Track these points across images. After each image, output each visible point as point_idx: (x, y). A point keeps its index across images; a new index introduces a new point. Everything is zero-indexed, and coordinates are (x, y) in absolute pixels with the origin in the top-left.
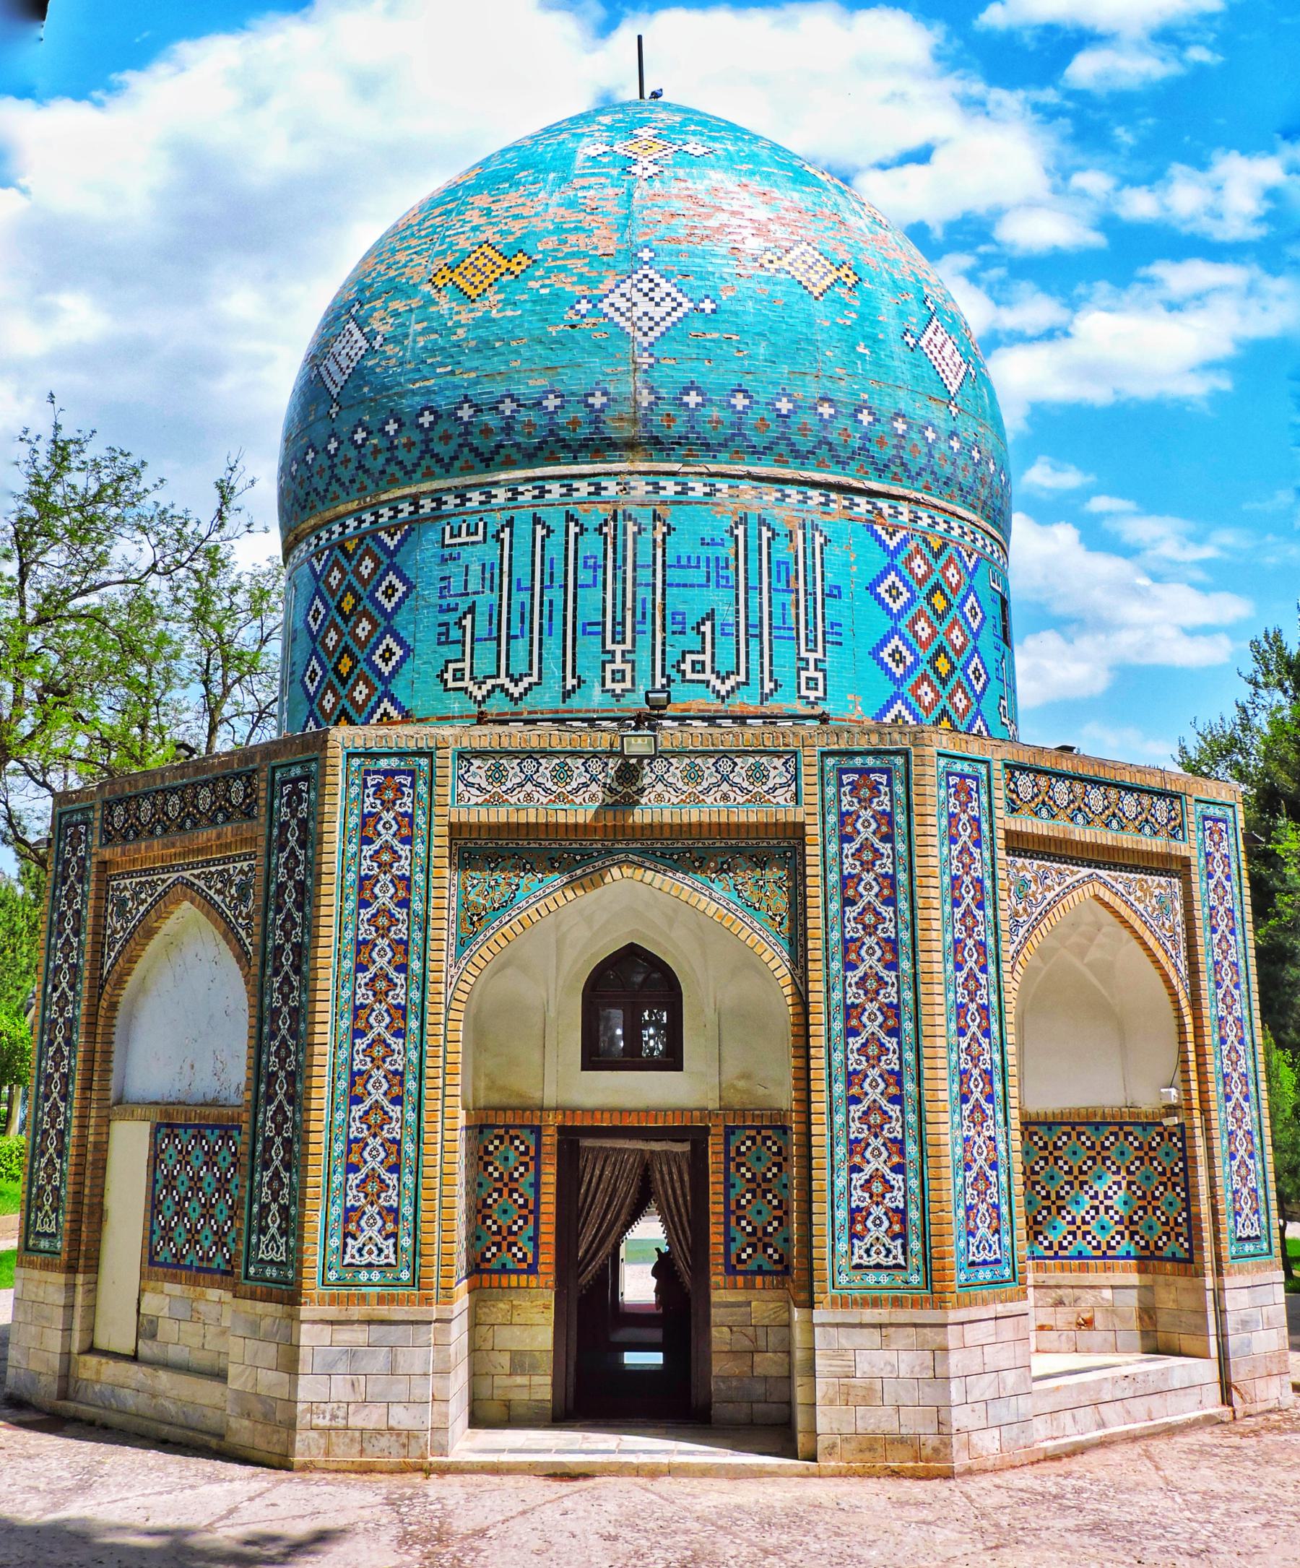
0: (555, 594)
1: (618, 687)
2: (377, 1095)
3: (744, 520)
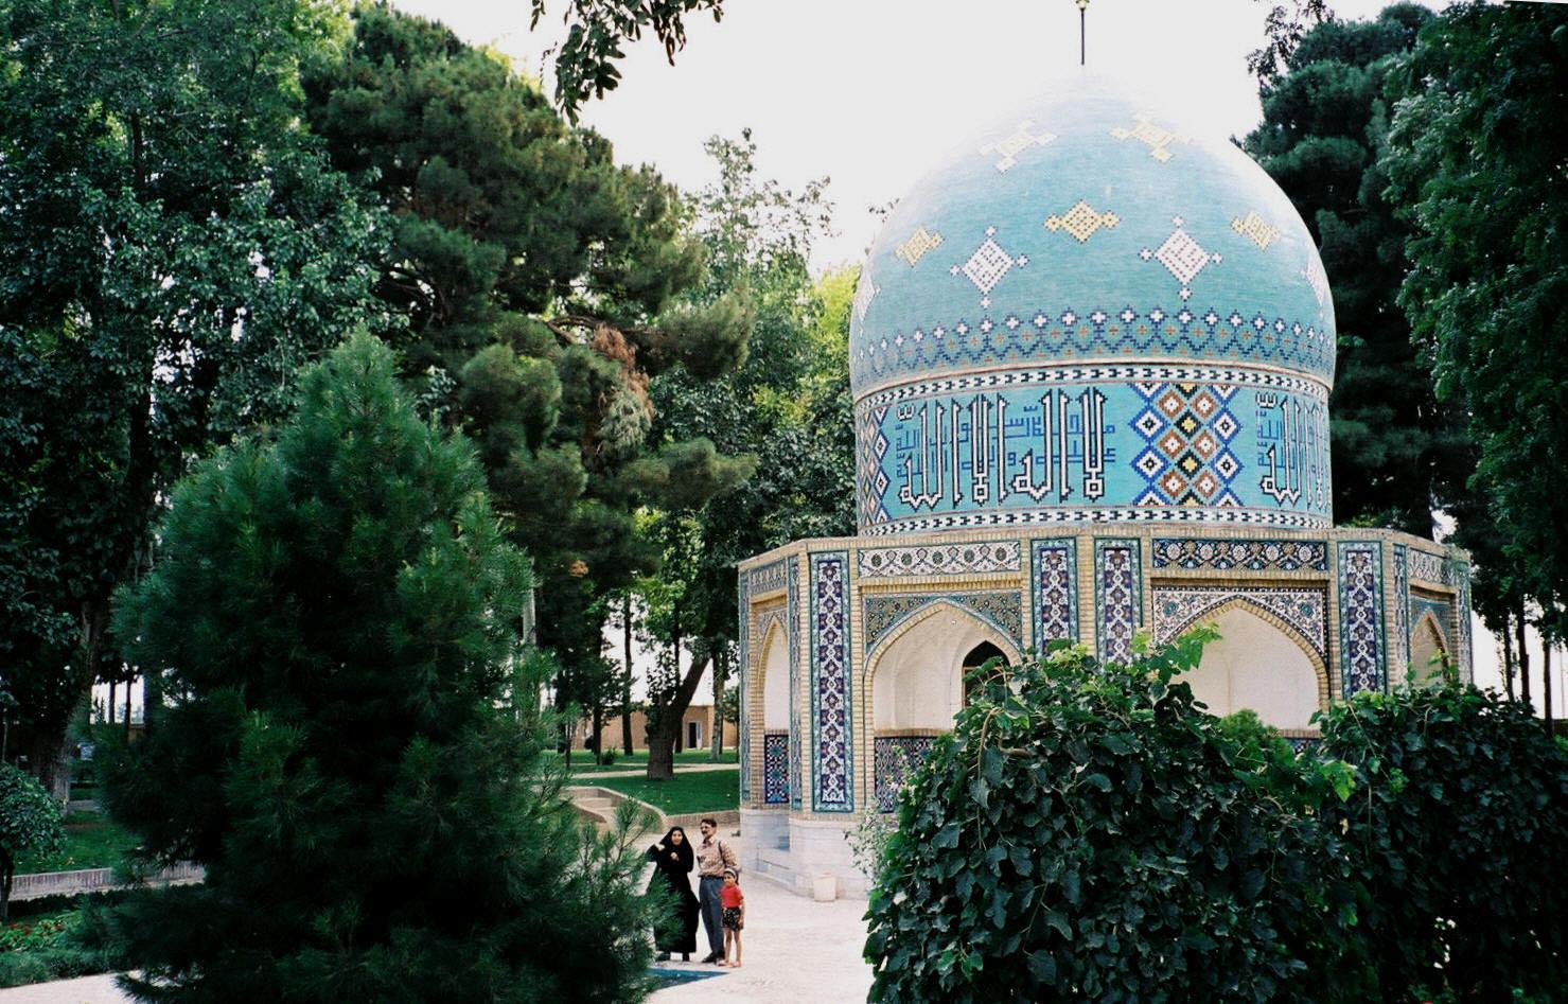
0: (947, 447)
1: (981, 498)
2: (832, 721)
3: (1050, 393)
